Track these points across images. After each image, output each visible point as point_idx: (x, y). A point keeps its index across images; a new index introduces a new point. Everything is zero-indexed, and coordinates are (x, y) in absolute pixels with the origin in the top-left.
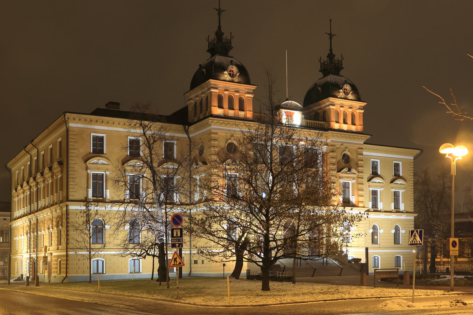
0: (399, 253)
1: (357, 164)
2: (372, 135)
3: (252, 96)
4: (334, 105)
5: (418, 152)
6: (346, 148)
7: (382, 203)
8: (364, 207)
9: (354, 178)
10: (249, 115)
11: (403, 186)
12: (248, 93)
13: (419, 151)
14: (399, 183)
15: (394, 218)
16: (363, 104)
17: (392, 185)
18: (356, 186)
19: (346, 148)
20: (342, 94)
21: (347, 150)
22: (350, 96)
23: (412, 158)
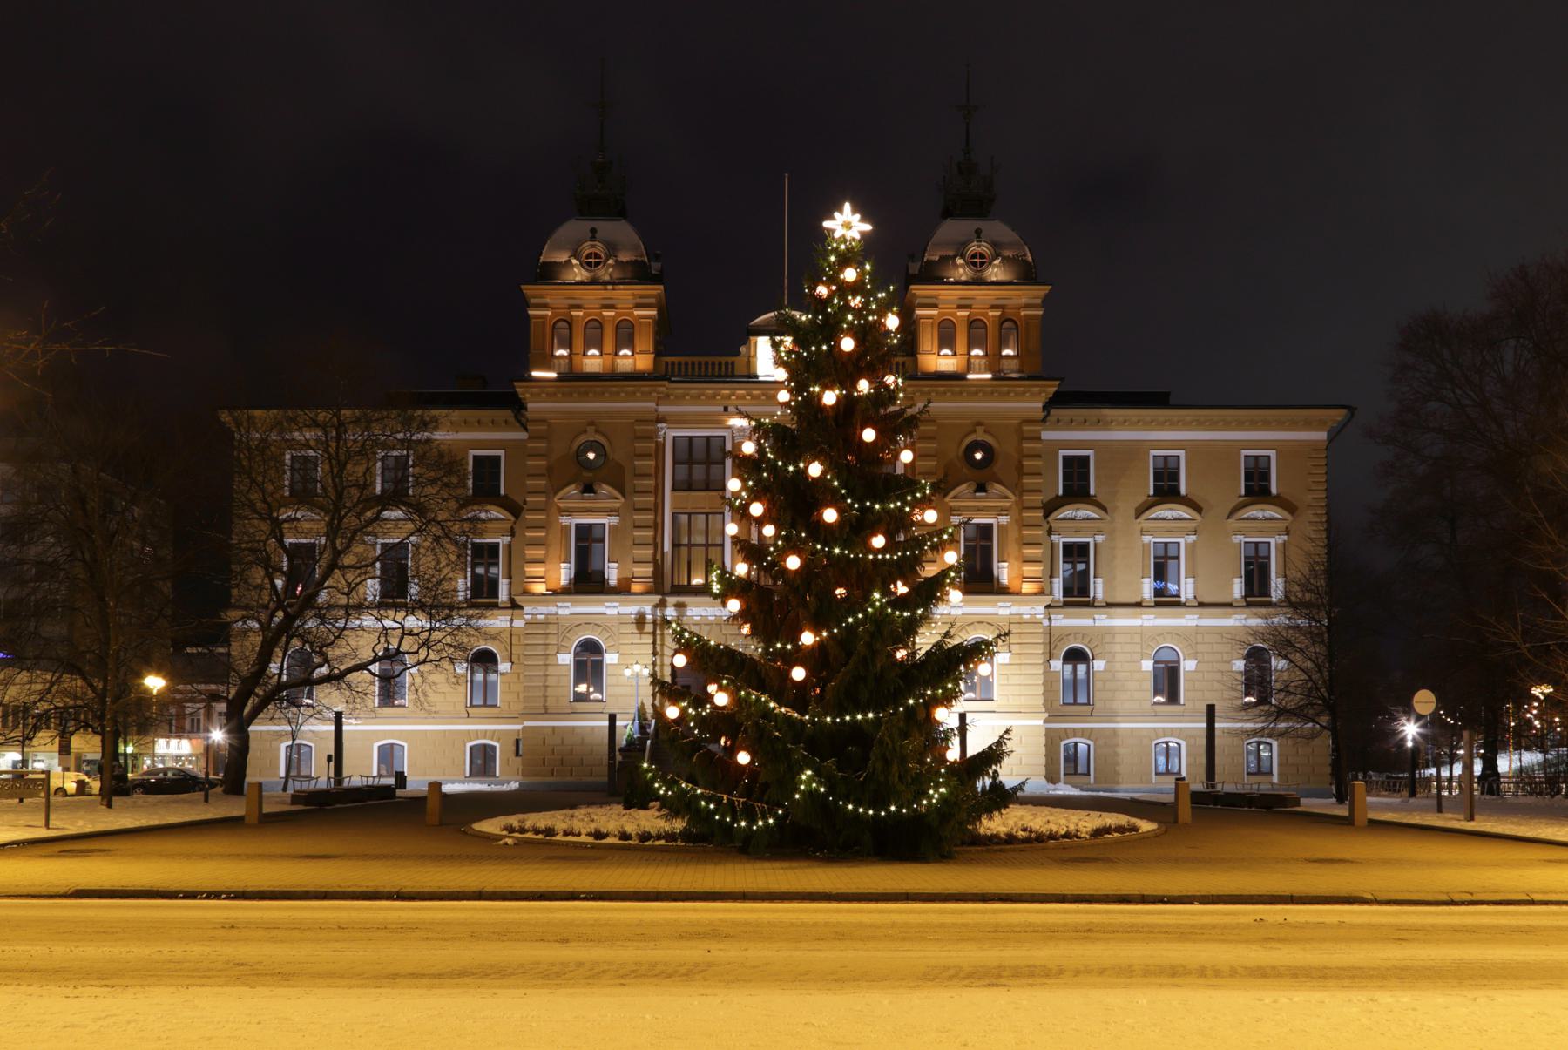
0: (492, 735)
1: (1021, 471)
2: (1062, 379)
3: (653, 312)
4: (935, 306)
5: (1339, 415)
6: (979, 424)
7: (1191, 580)
8: (1042, 593)
9: (1002, 511)
10: (644, 362)
11: (1285, 524)
12: (638, 306)
13: (1344, 411)
14: (1260, 515)
15: (1238, 624)
16: (1043, 290)
17: (1233, 523)
18: (1013, 534)
19: (979, 424)
20: (962, 272)
21: (980, 430)
22: (996, 272)
23: (1322, 436)
